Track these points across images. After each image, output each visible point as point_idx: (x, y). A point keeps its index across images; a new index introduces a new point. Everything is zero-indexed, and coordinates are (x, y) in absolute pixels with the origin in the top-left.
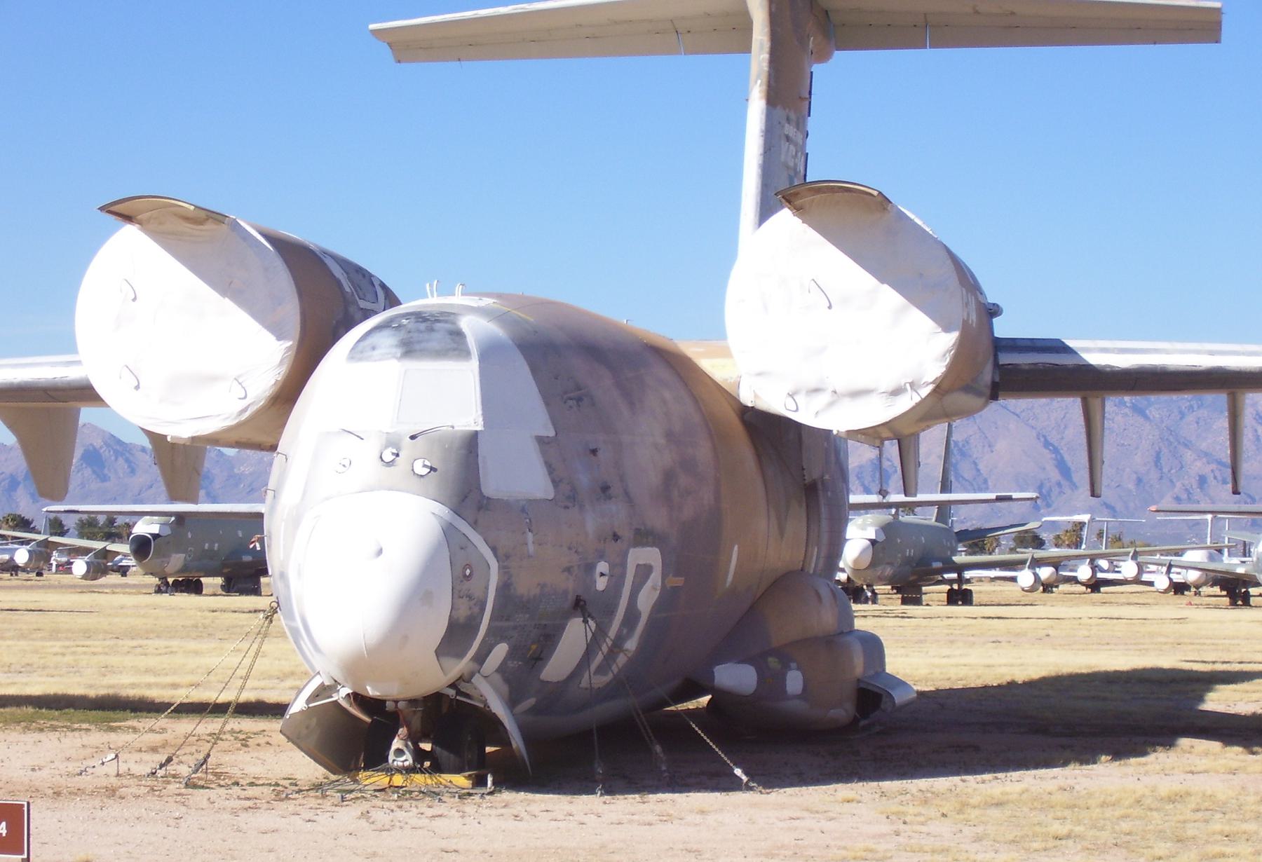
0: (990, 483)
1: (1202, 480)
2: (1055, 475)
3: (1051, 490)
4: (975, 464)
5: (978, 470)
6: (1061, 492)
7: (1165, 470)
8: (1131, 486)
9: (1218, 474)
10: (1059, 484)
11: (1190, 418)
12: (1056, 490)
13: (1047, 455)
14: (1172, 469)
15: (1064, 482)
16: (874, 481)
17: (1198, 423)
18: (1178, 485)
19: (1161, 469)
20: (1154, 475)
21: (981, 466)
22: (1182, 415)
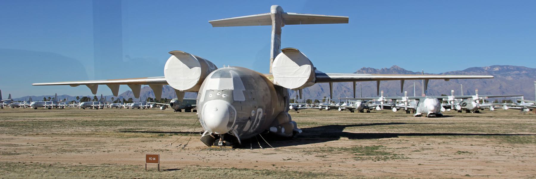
1: (345, 91)
2: (321, 90)
5: (308, 90)
6: (322, 93)
7: (339, 89)
10: (322, 92)
12: (321, 93)
13: (320, 87)
15: (323, 92)
20: (337, 90)
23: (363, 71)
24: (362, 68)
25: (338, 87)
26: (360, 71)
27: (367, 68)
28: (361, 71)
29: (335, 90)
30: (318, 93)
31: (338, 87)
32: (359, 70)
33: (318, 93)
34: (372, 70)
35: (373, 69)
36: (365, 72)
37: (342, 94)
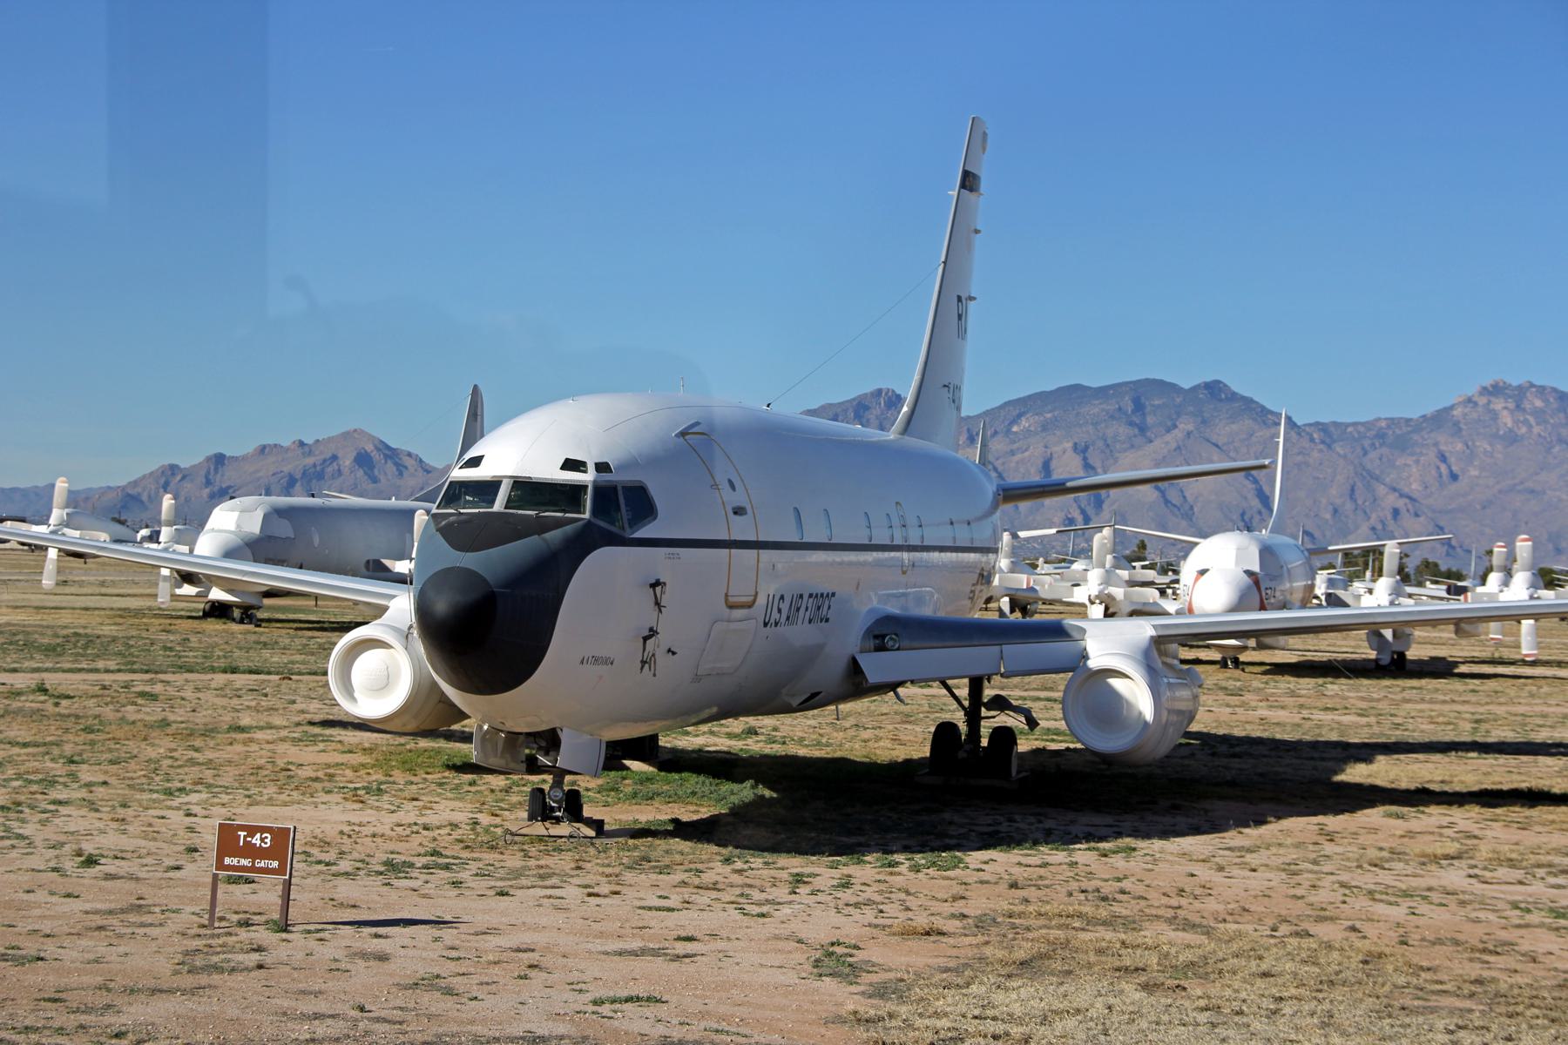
0: (1195, 509)
1: (1396, 513)
3: (1252, 518)
4: (1182, 491)
5: (1184, 497)
7: (1360, 502)
8: (1328, 516)
9: (1410, 507)
10: (1260, 513)
11: (1373, 455)
12: (1257, 518)
14: (1365, 501)
15: (1263, 510)
16: (1089, 504)
17: (1380, 459)
18: (1374, 516)
19: (1355, 501)
20: (1349, 506)
21: (1187, 494)
22: (1365, 453)
23: (1493, 399)
24: (1487, 382)
25: (1353, 490)
26: (1476, 404)
27: (1520, 387)
28: (1482, 401)
29: (1338, 501)
30: (1243, 520)
31: (1353, 490)
32: (1470, 394)
33: (1243, 514)
34: (1546, 401)
35: (1554, 390)
36: (1506, 408)
37: (1379, 527)
